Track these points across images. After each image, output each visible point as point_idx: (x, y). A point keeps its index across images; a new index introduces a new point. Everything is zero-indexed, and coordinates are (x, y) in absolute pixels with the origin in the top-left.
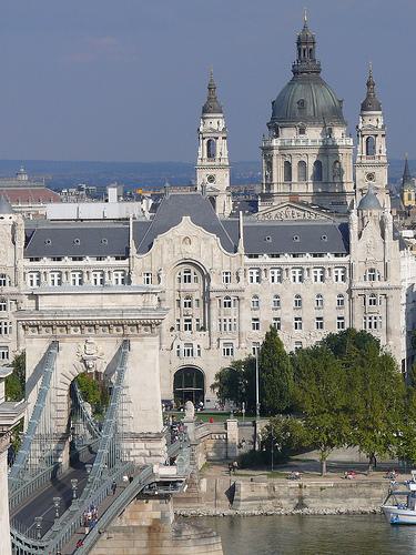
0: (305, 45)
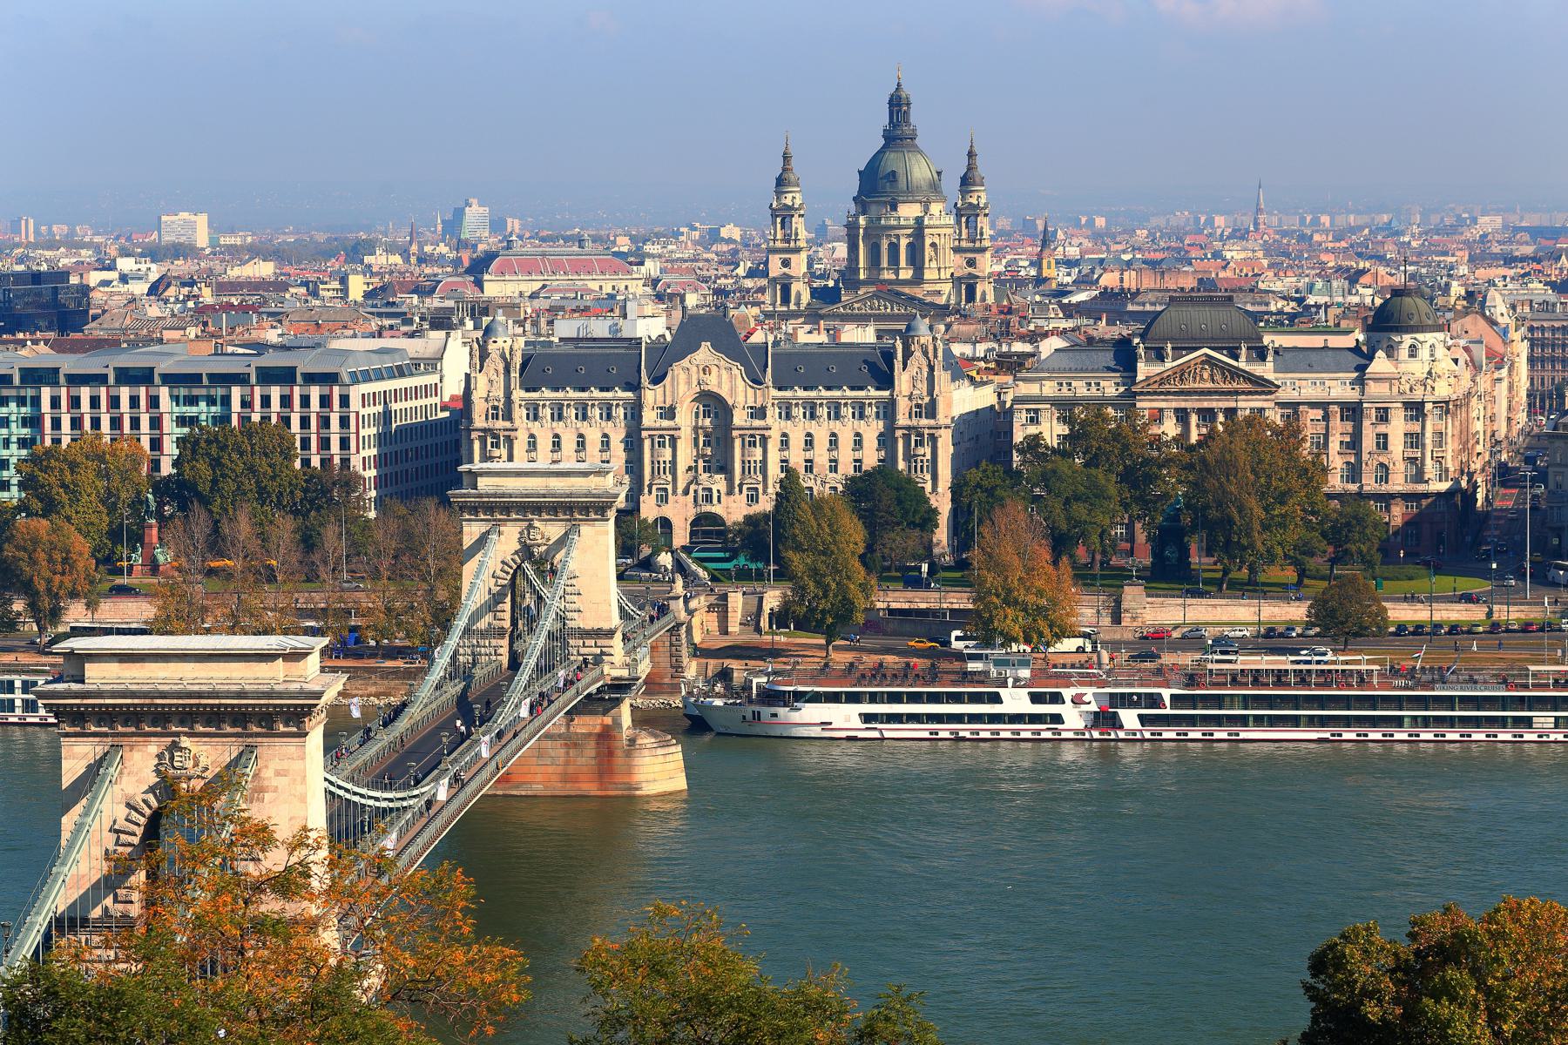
0: (898, 105)
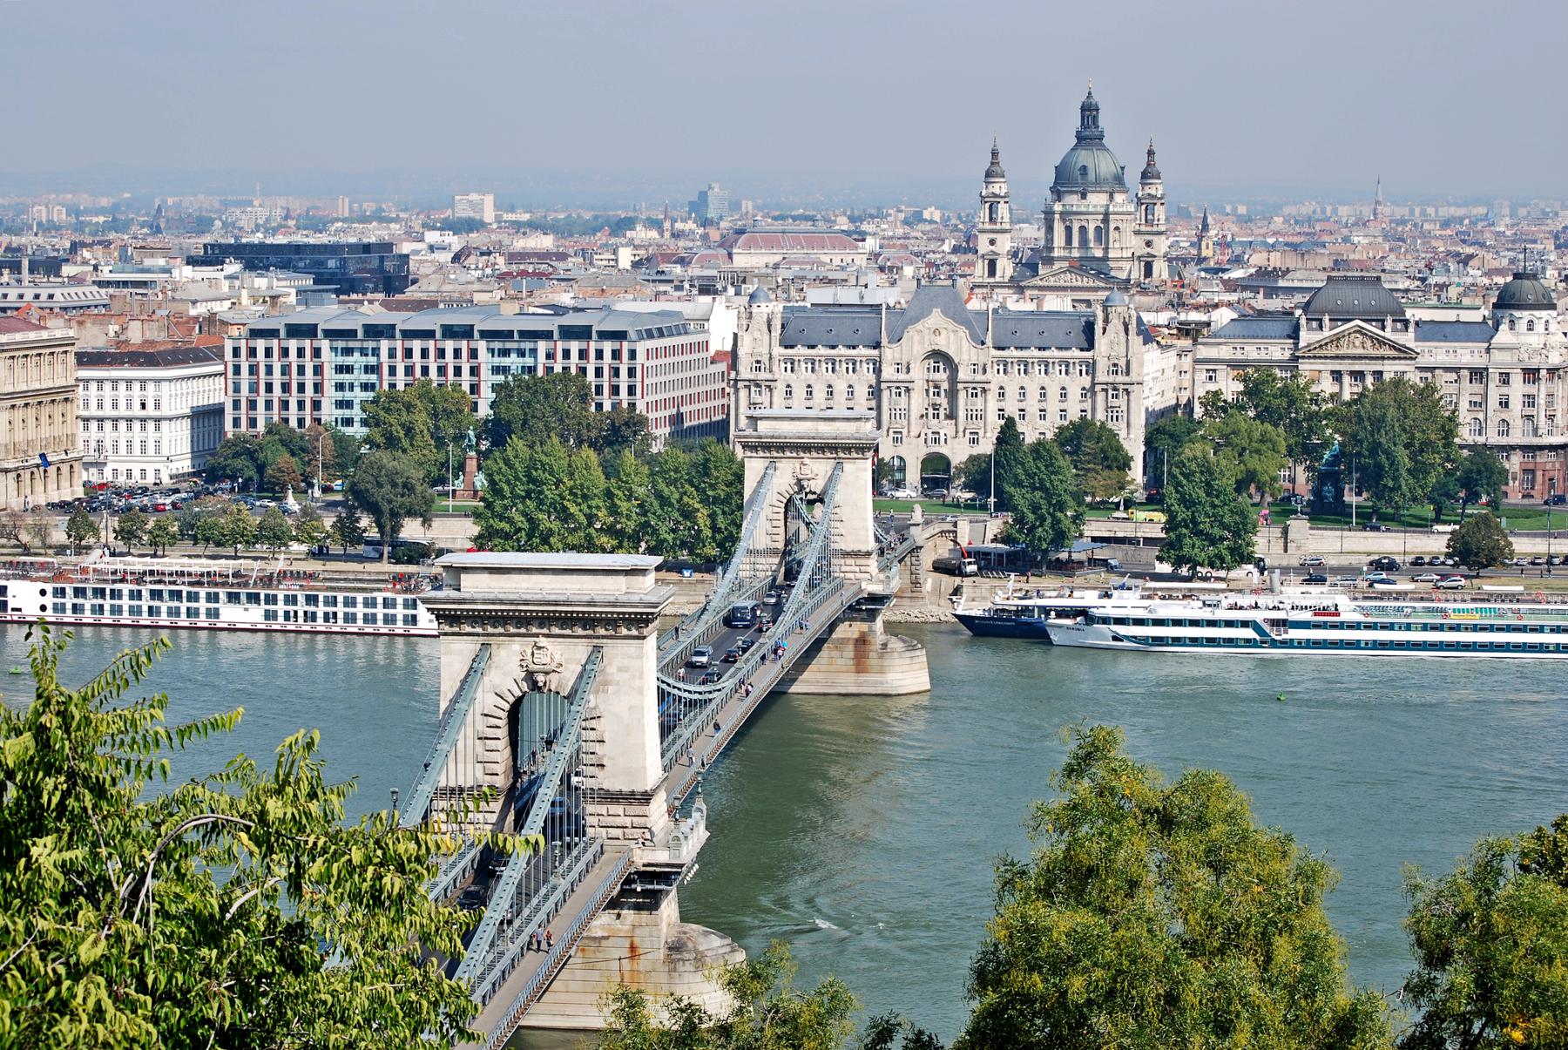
0: (1089, 111)
